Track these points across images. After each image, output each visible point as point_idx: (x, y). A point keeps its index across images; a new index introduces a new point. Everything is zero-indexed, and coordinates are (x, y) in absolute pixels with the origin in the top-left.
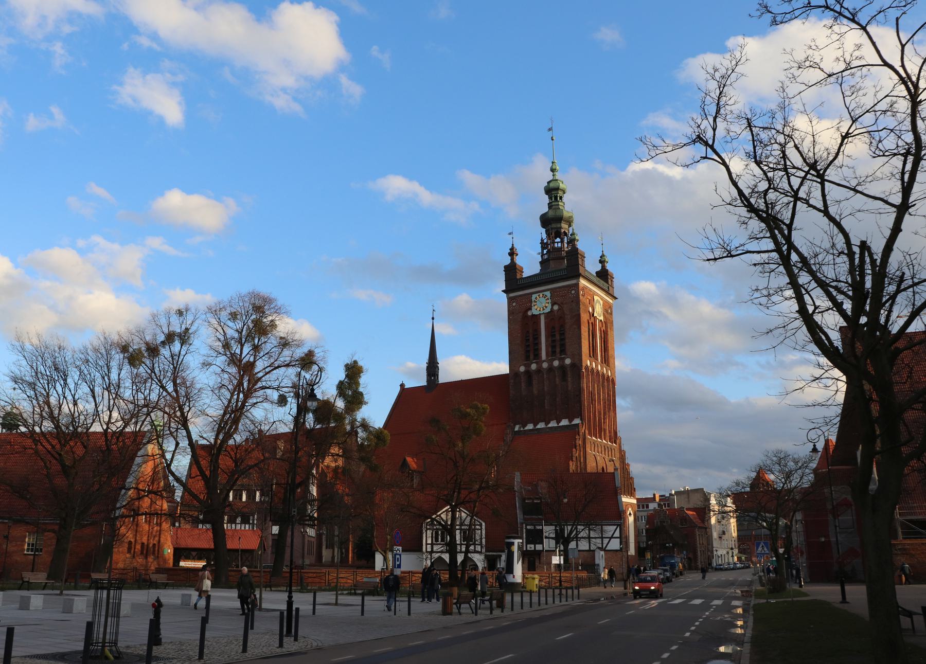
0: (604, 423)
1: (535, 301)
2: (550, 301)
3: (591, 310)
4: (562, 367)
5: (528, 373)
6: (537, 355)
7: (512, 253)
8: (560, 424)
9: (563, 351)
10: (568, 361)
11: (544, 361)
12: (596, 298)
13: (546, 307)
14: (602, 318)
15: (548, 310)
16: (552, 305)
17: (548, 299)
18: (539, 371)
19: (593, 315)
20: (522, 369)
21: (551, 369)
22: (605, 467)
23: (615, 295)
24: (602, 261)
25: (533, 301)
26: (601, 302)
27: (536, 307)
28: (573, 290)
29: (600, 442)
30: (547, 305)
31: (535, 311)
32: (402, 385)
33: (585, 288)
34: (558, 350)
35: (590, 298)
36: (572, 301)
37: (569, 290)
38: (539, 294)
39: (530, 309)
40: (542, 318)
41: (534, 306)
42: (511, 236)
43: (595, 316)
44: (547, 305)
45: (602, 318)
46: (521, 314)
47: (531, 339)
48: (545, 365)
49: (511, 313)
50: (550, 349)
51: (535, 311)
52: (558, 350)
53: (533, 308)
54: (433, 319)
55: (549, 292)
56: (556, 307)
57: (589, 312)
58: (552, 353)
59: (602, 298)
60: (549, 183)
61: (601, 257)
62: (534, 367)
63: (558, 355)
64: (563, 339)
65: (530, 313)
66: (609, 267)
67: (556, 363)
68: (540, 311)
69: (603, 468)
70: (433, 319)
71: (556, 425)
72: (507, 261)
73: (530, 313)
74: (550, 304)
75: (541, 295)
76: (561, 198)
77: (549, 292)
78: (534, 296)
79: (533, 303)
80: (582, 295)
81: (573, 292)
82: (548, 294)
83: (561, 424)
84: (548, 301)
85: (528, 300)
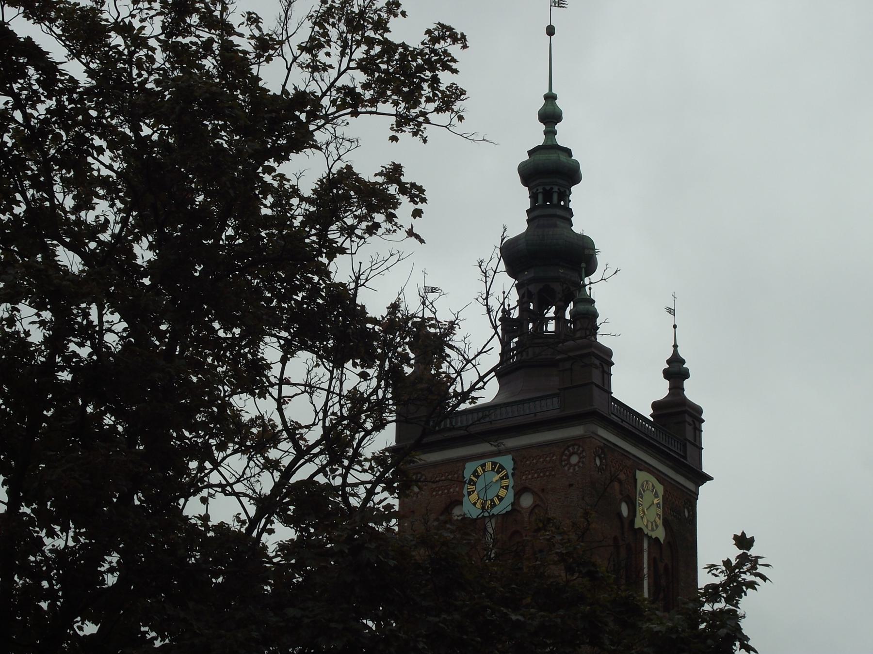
1: (471, 480)
2: (512, 484)
3: (624, 510)
12: (642, 476)
13: (501, 499)
14: (660, 533)
16: (518, 495)
19: (632, 522)
26: (660, 489)
27: (474, 497)
28: (574, 453)
30: (502, 493)
33: (607, 448)
36: (571, 485)
37: (563, 454)
38: (482, 462)
41: (469, 494)
43: (636, 526)
44: (502, 493)
45: (660, 533)
53: (465, 499)
55: (510, 457)
56: (527, 501)
57: (619, 515)
59: (661, 478)
60: (530, 153)
74: (511, 493)
75: (489, 466)
77: (510, 457)
81: (574, 459)
82: (507, 462)
84: (505, 483)
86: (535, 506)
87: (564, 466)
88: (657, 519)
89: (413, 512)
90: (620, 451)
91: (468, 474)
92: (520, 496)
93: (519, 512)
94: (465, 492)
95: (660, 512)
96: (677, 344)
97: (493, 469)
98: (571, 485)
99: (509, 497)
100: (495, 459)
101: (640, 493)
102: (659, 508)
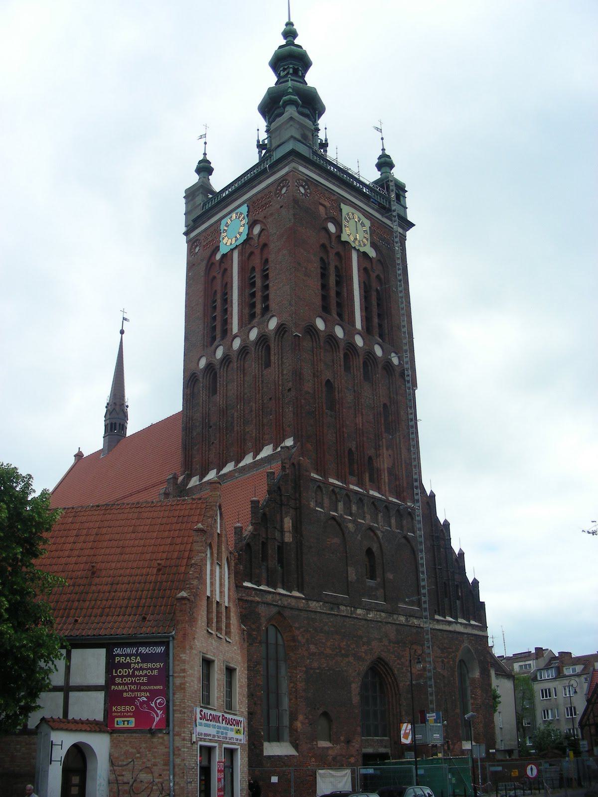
0: (378, 456)
1: (224, 230)
3: (332, 228)
4: (263, 339)
5: (210, 367)
6: (226, 331)
7: (204, 168)
8: (259, 457)
9: (266, 309)
10: (273, 324)
11: (236, 336)
12: (346, 209)
13: (240, 234)
15: (244, 237)
16: (251, 226)
17: (244, 218)
18: (226, 359)
19: (339, 237)
20: (203, 363)
21: (244, 350)
22: (375, 548)
23: (410, 218)
24: (385, 163)
25: (222, 231)
26: (368, 223)
28: (283, 187)
29: (357, 493)
31: (223, 250)
32: (79, 456)
33: (309, 182)
34: (258, 309)
35: (327, 204)
36: (281, 207)
38: (230, 216)
39: (217, 248)
40: (236, 255)
41: (223, 239)
42: (203, 140)
43: (343, 239)
46: (205, 262)
47: (219, 303)
48: (237, 344)
49: (191, 266)
50: (246, 311)
51: (223, 250)
52: (258, 309)
54: (122, 332)
56: (257, 230)
57: (326, 230)
58: (248, 319)
61: (380, 158)
62: (219, 353)
63: (256, 320)
64: (266, 287)
65: (218, 257)
66: (398, 173)
67: (253, 335)
68: (231, 244)
69: (369, 552)
70: (122, 332)
71: (252, 461)
72: (194, 179)
73: (218, 257)
74: (247, 226)
76: (296, 72)
78: (223, 222)
79: (223, 234)
80: (305, 195)
81: (284, 191)
82: (244, 209)
83: (259, 457)
84: (243, 222)
85: (215, 231)
86: (262, 231)
87: (278, 197)
88: (365, 240)
89: (194, 265)
90: (323, 187)
91: (223, 227)
92: (253, 228)
93: (252, 238)
94: (221, 239)
95: (368, 236)
96: (385, 148)
97: (236, 217)
98: (281, 207)
99: (244, 230)
100: (239, 210)
101: (346, 218)
102: (367, 233)
